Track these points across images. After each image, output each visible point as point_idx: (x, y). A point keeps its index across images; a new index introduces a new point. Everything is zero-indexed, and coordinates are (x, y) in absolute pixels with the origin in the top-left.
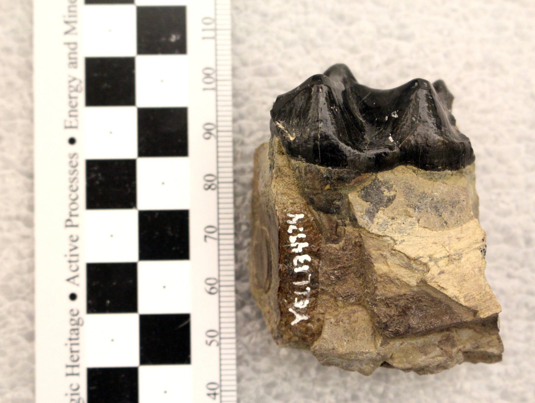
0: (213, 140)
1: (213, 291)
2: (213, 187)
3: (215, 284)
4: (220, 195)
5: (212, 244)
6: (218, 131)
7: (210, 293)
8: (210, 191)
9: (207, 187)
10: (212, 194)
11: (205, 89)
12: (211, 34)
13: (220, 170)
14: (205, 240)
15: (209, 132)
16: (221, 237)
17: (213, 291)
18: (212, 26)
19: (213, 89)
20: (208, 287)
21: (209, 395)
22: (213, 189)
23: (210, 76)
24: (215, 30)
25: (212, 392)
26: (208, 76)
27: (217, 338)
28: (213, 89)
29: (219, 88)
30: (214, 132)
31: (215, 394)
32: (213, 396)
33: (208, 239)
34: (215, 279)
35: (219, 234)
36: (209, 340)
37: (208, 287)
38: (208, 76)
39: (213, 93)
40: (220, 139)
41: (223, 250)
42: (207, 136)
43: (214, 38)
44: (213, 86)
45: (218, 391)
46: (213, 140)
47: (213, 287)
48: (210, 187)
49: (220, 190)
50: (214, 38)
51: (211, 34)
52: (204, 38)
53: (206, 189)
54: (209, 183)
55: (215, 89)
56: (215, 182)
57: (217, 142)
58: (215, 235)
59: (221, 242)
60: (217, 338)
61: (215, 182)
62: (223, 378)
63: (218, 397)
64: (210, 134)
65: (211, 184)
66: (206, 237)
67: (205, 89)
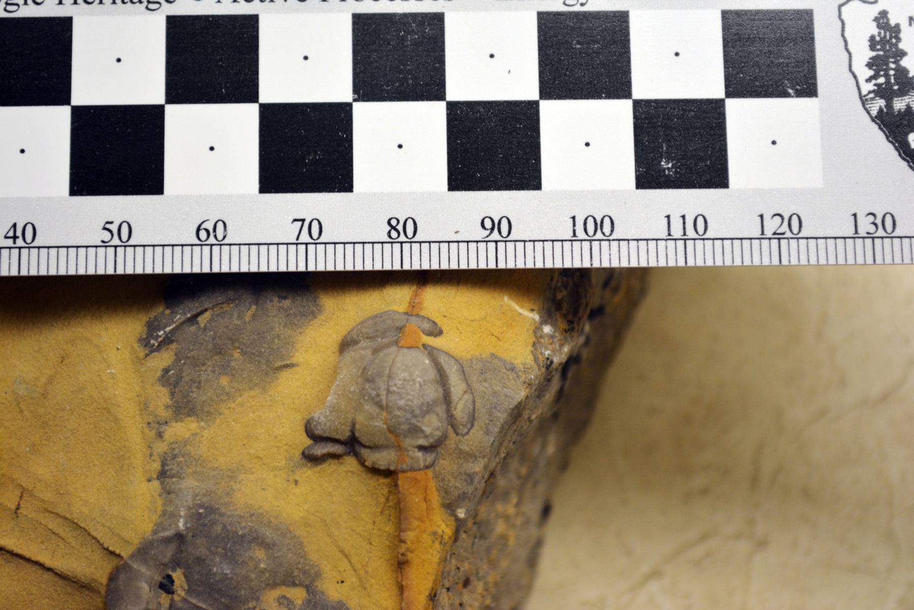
0: (482, 234)
1: (203, 234)
2: (394, 234)
3: (215, 237)
4: (378, 247)
9: (394, 222)
12: (677, 232)
13: (425, 246)
14: (295, 220)
15: (496, 226)
17: (203, 234)
18: (691, 233)
20: (209, 226)
21: (15, 226)
23: (599, 227)
25: (19, 233)
26: (599, 225)
27: (116, 241)
29: (577, 245)
30: (495, 236)
31: (15, 238)
32: (11, 234)
34: (224, 237)
36: (114, 228)
37: (209, 226)
40: (482, 246)
42: (488, 224)
43: (670, 237)
45: (20, 243)
46: (482, 234)
47: (208, 234)
49: (387, 247)
50: (670, 237)
51: (677, 232)
52: (668, 217)
53: (389, 223)
54: (400, 228)
56: (402, 238)
58: (305, 237)
59: (292, 248)
60: (116, 241)
61: (402, 238)
62: (44, 251)
63: (9, 243)
64: (492, 229)
65: (399, 230)
66: (303, 220)
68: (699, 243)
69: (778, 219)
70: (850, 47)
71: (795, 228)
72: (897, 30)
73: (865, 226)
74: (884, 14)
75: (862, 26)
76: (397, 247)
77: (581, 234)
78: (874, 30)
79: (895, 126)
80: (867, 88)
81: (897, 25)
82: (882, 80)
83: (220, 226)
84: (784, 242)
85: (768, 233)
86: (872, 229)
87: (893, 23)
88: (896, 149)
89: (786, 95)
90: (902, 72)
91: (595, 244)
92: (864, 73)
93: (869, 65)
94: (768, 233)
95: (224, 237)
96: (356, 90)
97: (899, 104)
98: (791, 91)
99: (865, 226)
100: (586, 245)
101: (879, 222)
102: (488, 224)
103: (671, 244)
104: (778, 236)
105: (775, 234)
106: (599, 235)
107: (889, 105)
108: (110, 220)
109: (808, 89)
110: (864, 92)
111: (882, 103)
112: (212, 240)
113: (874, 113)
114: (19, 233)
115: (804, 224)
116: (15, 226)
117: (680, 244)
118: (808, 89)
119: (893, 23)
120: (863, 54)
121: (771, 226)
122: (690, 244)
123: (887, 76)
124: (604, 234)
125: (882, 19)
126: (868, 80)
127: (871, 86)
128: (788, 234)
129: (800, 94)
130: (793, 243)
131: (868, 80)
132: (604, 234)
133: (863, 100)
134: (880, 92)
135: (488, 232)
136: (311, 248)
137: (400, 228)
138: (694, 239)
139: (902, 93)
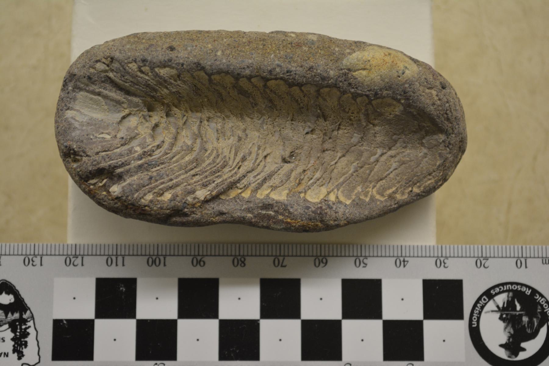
0: (206, 259)
1: (324, 261)
2: (243, 259)
5: (287, 261)
6: (199, 255)
7: (326, 263)
8: (246, 262)
9: (243, 265)
10: (248, 260)
11: (165, 265)
12: (120, 259)
14: (285, 266)
15: (199, 262)
16: (282, 254)
18: (114, 258)
19: (165, 258)
20: (322, 265)
21: (404, 266)
22: (245, 260)
24: (117, 255)
25: (402, 263)
26: (154, 262)
27: (361, 259)
28: (165, 258)
29: (164, 253)
30: (199, 258)
31: (404, 261)
32: (406, 263)
33: (284, 264)
34: (315, 260)
35: (280, 256)
37: (322, 265)
38: (154, 262)
39: (168, 258)
41: (288, 253)
42: (202, 263)
44: (162, 258)
45: (402, 259)
46: (206, 259)
48: (243, 262)
49: (246, 254)
51: (120, 259)
53: (245, 265)
54: (240, 262)
55: (165, 256)
56: (239, 258)
57: (207, 256)
58: (281, 259)
63: (406, 259)
64: (200, 261)
66: (282, 266)
67: (165, 265)
68: (111, 253)
69: (75, 264)
70: (36, 342)
71: (68, 259)
72: (14, 351)
73: (37, 260)
74: (19, 358)
75: (30, 353)
76: (242, 254)
77: (162, 258)
78: (25, 351)
79: (19, 305)
80: (30, 324)
81: (14, 353)
82: (23, 327)
83: (317, 264)
84: (74, 253)
85: (80, 258)
86: (34, 259)
87: (16, 354)
88: (20, 295)
89: (67, 320)
90: (14, 331)
91: (156, 253)
92: (31, 331)
93: (28, 334)
94: (80, 258)
95: (315, 260)
96: (258, 325)
97: (17, 315)
98: (65, 322)
99: (37, 260)
100: (160, 253)
101: (31, 262)
102: (202, 263)
103: (123, 253)
104: (76, 256)
105: (77, 257)
106: (154, 257)
107: (21, 315)
108: (364, 268)
109: (57, 323)
110: (32, 321)
111: (25, 316)
112: (321, 258)
113: (28, 312)
114: (402, 263)
115: (64, 261)
116: (404, 266)
117: (119, 253)
118: (57, 323)
119: (16, 354)
120: (31, 340)
121: (78, 261)
122: (115, 253)
123: (21, 329)
124: (152, 258)
125: (21, 356)
126: (29, 327)
127: (29, 324)
128: (71, 257)
129: (61, 321)
130: (69, 253)
131: (29, 327)
132: (152, 258)
133: (32, 317)
134: (25, 321)
135: (203, 259)
136: (278, 254)
137: (240, 262)
138: (113, 255)
139: (15, 321)
